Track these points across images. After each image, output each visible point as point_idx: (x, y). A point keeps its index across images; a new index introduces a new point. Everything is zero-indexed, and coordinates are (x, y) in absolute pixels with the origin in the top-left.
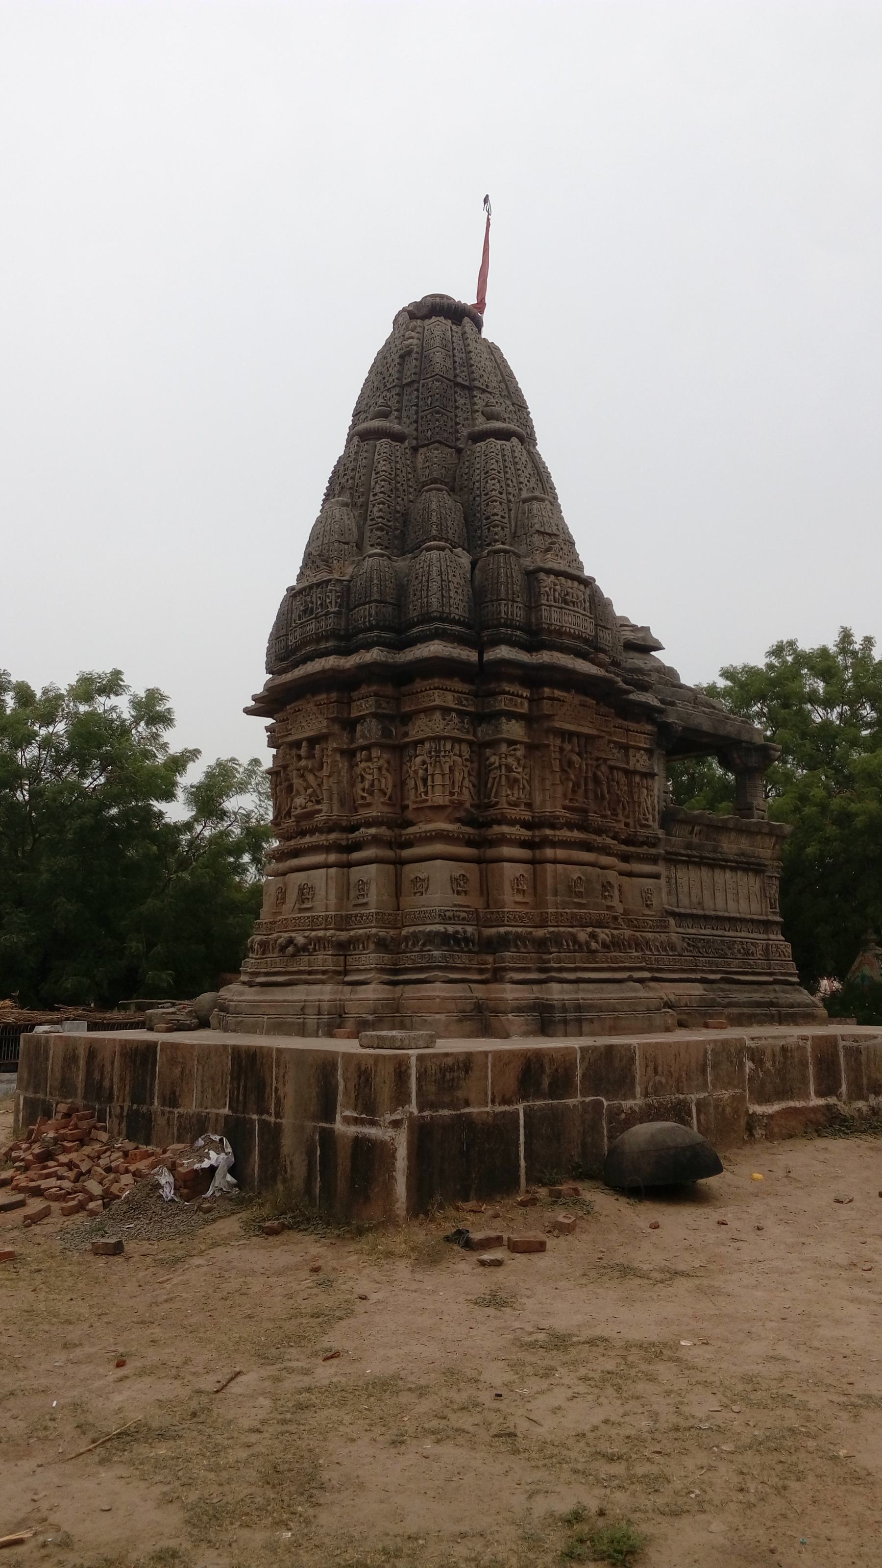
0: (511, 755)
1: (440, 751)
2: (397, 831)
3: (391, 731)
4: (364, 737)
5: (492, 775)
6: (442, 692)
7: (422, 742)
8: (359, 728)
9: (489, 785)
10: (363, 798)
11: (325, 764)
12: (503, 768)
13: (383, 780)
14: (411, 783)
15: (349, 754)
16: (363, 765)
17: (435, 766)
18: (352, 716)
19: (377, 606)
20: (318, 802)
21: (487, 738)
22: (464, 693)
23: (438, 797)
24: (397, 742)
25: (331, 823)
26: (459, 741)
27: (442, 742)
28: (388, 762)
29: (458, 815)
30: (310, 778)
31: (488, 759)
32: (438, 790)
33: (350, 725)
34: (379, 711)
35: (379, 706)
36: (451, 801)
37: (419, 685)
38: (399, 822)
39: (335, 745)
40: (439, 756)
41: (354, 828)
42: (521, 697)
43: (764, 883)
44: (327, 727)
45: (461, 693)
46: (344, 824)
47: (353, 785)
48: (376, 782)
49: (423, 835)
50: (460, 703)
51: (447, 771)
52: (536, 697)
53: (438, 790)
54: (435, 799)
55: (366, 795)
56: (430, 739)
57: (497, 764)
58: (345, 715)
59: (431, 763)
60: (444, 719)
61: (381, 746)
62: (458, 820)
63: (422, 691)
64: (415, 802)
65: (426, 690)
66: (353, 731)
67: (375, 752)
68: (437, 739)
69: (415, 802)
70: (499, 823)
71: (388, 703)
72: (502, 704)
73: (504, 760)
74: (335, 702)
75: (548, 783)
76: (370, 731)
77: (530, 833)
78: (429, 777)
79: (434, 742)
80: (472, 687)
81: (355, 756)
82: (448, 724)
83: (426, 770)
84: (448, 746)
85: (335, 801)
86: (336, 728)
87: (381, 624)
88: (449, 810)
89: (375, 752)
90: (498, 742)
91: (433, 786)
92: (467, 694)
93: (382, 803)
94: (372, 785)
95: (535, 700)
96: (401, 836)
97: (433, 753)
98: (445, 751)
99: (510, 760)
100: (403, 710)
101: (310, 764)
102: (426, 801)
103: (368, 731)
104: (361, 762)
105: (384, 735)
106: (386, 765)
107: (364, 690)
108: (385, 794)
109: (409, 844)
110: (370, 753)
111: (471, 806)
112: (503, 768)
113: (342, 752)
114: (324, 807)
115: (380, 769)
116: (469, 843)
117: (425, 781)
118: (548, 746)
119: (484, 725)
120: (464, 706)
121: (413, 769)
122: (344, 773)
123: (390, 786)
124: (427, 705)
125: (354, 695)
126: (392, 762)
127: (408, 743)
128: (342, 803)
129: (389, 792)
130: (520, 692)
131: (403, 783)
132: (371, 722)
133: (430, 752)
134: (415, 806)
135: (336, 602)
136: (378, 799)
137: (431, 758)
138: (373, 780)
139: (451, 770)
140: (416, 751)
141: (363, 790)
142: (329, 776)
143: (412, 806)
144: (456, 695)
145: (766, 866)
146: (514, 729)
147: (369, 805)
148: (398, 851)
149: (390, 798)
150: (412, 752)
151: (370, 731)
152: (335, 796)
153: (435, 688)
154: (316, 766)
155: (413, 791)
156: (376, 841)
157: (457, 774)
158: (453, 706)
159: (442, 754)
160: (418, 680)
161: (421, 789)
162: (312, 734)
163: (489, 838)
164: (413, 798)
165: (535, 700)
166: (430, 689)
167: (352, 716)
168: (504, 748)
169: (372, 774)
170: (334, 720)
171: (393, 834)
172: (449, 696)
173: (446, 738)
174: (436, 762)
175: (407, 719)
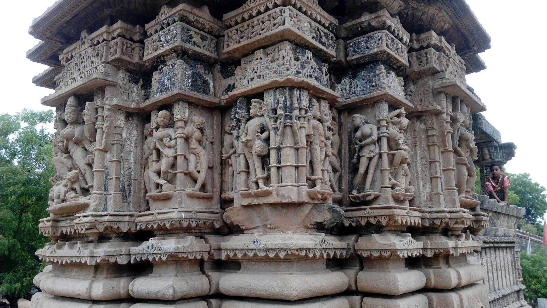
0: (394, 124)
1: (292, 109)
3: (206, 82)
4: (163, 88)
5: (366, 152)
6: (295, 11)
7: (260, 95)
8: (156, 76)
9: (362, 170)
10: (158, 186)
11: (99, 131)
12: (384, 142)
13: (192, 158)
14: (238, 164)
15: (142, 117)
16: (162, 132)
17: (283, 133)
18: (145, 58)
20: (86, 191)
21: (353, 98)
22: (323, 25)
24: (216, 100)
25: (101, 228)
26: (317, 95)
27: (296, 93)
28: (201, 130)
29: (319, 219)
30: (77, 153)
31: (357, 129)
32: (289, 174)
33: (142, 75)
34: (188, 46)
36: (312, 197)
38: (217, 226)
39: (115, 101)
40: (291, 118)
42: (401, 40)
43: (514, 257)
44: (106, 74)
46: (125, 228)
47: (145, 167)
48: (180, 160)
50: (318, 38)
51: (303, 142)
52: (416, 46)
53: (289, 174)
54: (283, 191)
55: (161, 182)
56: (276, 87)
57: (375, 137)
58: (136, 60)
59: (276, 129)
60: (297, 59)
61: (192, 104)
62: (320, 227)
63: (259, 13)
64: (249, 196)
66: (147, 85)
67: (181, 112)
68: (289, 86)
69: (249, 196)
71: (203, 38)
72: (381, 43)
73: (384, 130)
74: (119, 36)
75: (439, 167)
76: (175, 78)
77: (419, 245)
78: (273, 154)
79: (283, 93)
80: (333, 20)
81: (148, 120)
82: (303, 67)
83: (267, 140)
84: (305, 102)
85: (112, 190)
86: (121, 78)
88: (307, 209)
89: (181, 112)
90: (373, 102)
91: (279, 168)
92: (327, 28)
93: (191, 196)
94: (173, 166)
95: (416, 50)
97: (280, 112)
98: (300, 109)
99: (394, 131)
100: (226, 50)
101: (77, 131)
102: (268, 194)
103: (170, 79)
104: (157, 128)
105: (194, 85)
106: (198, 134)
108: (195, 181)
109: (231, 265)
110: (172, 115)
111: (335, 201)
112: (384, 142)
113: (129, 115)
114: (92, 200)
115: (187, 139)
116: (336, 263)
117: (264, 159)
118: (438, 114)
119: (346, 82)
120: (323, 44)
121: (243, 139)
122: (130, 147)
123: (204, 168)
124: (269, 33)
125: (150, 27)
126: (208, 131)
129: (201, 178)
130: (401, 33)
131: (224, 163)
132: (173, 65)
133: (275, 111)
134: (246, 202)
136: (183, 188)
138: (175, 157)
139: (309, 143)
140: (248, 111)
141: (159, 173)
142: (105, 151)
143: (239, 202)
144: (314, 24)
145: (514, 243)
146: (392, 85)
147: (167, 198)
148: (214, 275)
149: (203, 187)
150: (243, 112)
151: (175, 78)
154: (87, 134)
155: (243, 177)
156: (176, 261)
158: (309, 39)
159: (296, 113)
161: (260, 174)
162: (79, 83)
165: (416, 50)
167: (145, 58)
169: (174, 147)
170: (118, 64)
171: (206, 248)
173: (302, 87)
174: (285, 127)
175: (229, 65)
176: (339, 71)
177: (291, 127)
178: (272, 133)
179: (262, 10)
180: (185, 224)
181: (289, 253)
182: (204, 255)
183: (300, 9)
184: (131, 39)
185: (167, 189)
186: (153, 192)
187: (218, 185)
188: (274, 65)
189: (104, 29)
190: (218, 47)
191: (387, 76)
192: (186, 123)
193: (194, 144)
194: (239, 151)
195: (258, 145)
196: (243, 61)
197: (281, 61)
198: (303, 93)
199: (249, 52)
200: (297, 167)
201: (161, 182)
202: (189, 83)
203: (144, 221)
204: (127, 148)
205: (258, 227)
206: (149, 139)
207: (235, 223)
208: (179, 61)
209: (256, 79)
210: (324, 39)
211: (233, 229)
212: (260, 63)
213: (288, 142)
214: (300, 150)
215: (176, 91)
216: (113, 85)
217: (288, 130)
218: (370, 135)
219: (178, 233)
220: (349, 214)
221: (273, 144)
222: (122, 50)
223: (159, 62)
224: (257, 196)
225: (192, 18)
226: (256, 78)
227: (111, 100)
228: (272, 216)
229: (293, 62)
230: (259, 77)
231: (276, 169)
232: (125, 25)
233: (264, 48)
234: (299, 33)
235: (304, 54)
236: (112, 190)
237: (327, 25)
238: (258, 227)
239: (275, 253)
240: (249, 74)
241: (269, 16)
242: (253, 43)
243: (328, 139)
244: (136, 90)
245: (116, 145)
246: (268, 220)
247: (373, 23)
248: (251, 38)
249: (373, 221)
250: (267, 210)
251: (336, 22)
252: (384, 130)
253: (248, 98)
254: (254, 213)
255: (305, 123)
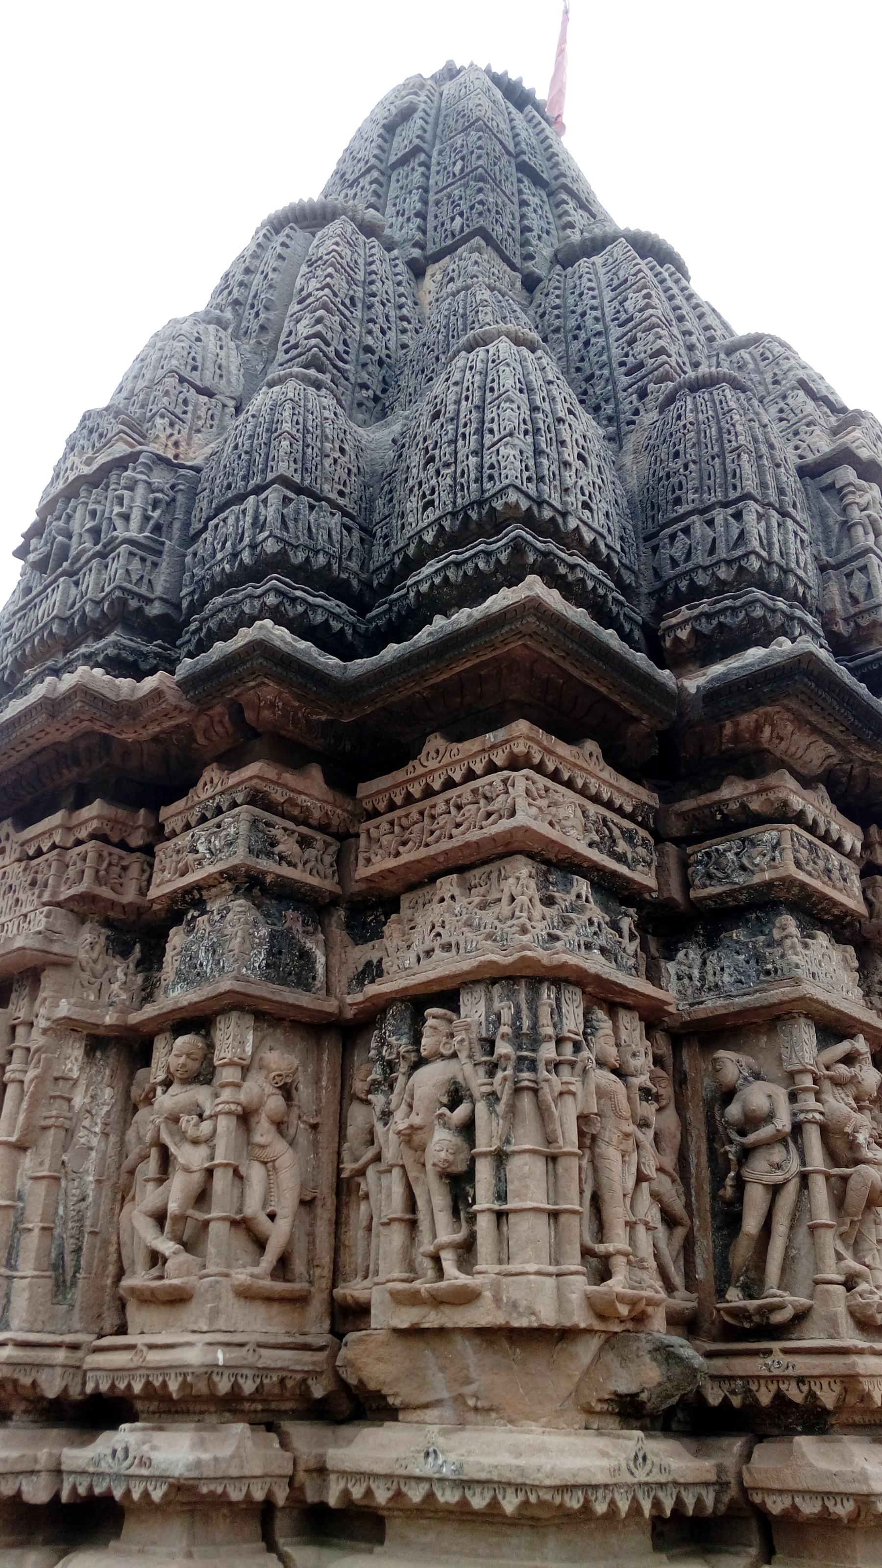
0: (838, 1083)
1: (535, 1041)
2: (304, 1436)
3: (306, 956)
4: (191, 975)
5: (760, 1169)
6: (542, 781)
7: (447, 996)
8: (177, 938)
9: (751, 1224)
10: (156, 1258)
12: (813, 1138)
13: (256, 1174)
14: (385, 1195)
17: (512, 1109)
18: (154, 893)
19: (286, 501)
21: (712, 1004)
22: (620, 811)
23: (532, 1281)
24: (331, 1006)
26: (606, 998)
27: (547, 995)
28: (287, 1091)
29: (624, 1384)
31: (728, 1095)
32: (529, 1232)
33: (140, 935)
34: (264, 864)
35: (267, 847)
36: (601, 1311)
37: (439, 757)
38: (318, 1391)
39: (64, 1009)
40: (533, 1066)
41: (99, 1412)
42: (837, 845)
44: (48, 934)
45: (608, 804)
47: (123, 1194)
48: (221, 1182)
49: (448, 1497)
50: (607, 845)
51: (569, 1138)
53: (529, 1232)
54: (513, 1290)
55: (166, 1246)
57: (783, 1122)
58: (130, 895)
59: (493, 1097)
60: (549, 901)
61: (265, 1016)
62: (629, 1411)
63: (450, 784)
64: (413, 1299)
65: (470, 775)
66: (151, 960)
67: (233, 1039)
68: (527, 978)
69: (413, 1299)
70: (815, 1420)
71: (304, 842)
72: (779, 857)
73: (809, 1101)
74: (93, 836)
76: (223, 948)
78: (484, 1171)
79: (511, 995)
80: (644, 795)
82: (566, 923)
83: (468, 1129)
84: (573, 1019)
86: (85, 944)
87: (299, 557)
88: (586, 1351)
89: (233, 1039)
90: (772, 1020)
91: (501, 1216)
92: (631, 817)
93: (247, 1294)
94: (202, 1198)
96: (321, 1471)
97: (503, 1048)
99: (838, 1104)
100: (362, 872)
102: (466, 1297)
103: (213, 949)
104: (167, 1084)
105: (274, 969)
106: (275, 1103)
107: (213, 783)
108: (260, 1244)
110: (210, 1047)
111: (675, 1320)
112: (813, 1138)
113: (97, 1043)
115: (245, 1118)
117: (459, 1184)
119: (690, 955)
120: (621, 858)
121: (400, 1122)
122: (89, 1135)
123: (286, 1204)
124: (474, 835)
125: (172, 814)
126: (304, 1093)
127: (371, 1018)
128: (60, 1278)
129: (278, 1234)
130: (834, 827)
131: (345, 1189)
133: (489, 1044)
134: (405, 1318)
135: (147, 518)
137: (492, 1069)
138: (209, 1173)
139: (588, 1140)
140: (416, 1040)
141: (160, 1218)
143: (385, 1316)
144: (593, 809)
146: (824, 970)
147: (178, 1299)
149: (283, 1267)
150: (401, 1043)
151: (223, 948)
152: (31, 1243)
153: (514, 764)
155: (396, 1237)
157: (611, 1154)
158: (582, 848)
159: (548, 1051)
160: (435, 742)
161: (447, 1232)
163: (776, 1506)
164: (390, 1269)
166: (492, 768)
167: (154, 893)
168: (804, 1045)
169: (209, 1140)
170: (83, 908)
172: (569, 806)
173: (562, 978)
174: (518, 1090)
175: (371, 910)
176: (667, 926)
177: (535, 1091)
178: (481, 1108)
179: (457, 777)
180: (224, 1386)
181: (533, 1499)
182: (276, 1489)
183: (555, 776)
184: (123, 845)
185: (179, 1269)
186: (139, 1278)
187: (325, 1258)
188: (488, 917)
189: (56, 818)
190: (342, 863)
191: (806, 946)
192: (245, 1070)
193: (264, 1132)
194: (390, 1155)
195: (441, 1143)
196: (405, 901)
197: (505, 908)
198: (568, 995)
199: (423, 878)
200: (554, 1215)
201: (166, 1246)
202: (260, 959)
203: (109, 1366)
204: (81, 1137)
205: (438, 1403)
206: (143, 1113)
207: (372, 1386)
208: (240, 904)
209: (438, 953)
210: (622, 846)
211: (361, 1406)
212: (450, 910)
213: (527, 1138)
214: (562, 1163)
215: (226, 985)
216: (64, 963)
217: (526, 1102)
218: (770, 1117)
219: (201, 1413)
220: (720, 1365)
221: (483, 1144)
222: (97, 871)
223: (189, 903)
224: (437, 1301)
225: (278, 796)
226: (438, 951)
227: (55, 1003)
228: (483, 1372)
229: (539, 909)
230: (447, 947)
231: (493, 1217)
232: (110, 811)
233: (461, 870)
234: (554, 834)
235: (567, 886)
236: (27, 1267)
237: (629, 809)
238: (438, 1403)
239: (488, 1496)
240: (421, 939)
241: (475, 791)
242: (433, 858)
243: (644, 1124)
244: (122, 975)
245: (52, 1131)
246: (468, 1381)
247: (755, 805)
248: (427, 845)
249: (796, 1394)
250: (466, 1348)
251: (652, 799)
252: (809, 1101)
253: (418, 1003)
254: (428, 1357)
255: (573, 1079)
